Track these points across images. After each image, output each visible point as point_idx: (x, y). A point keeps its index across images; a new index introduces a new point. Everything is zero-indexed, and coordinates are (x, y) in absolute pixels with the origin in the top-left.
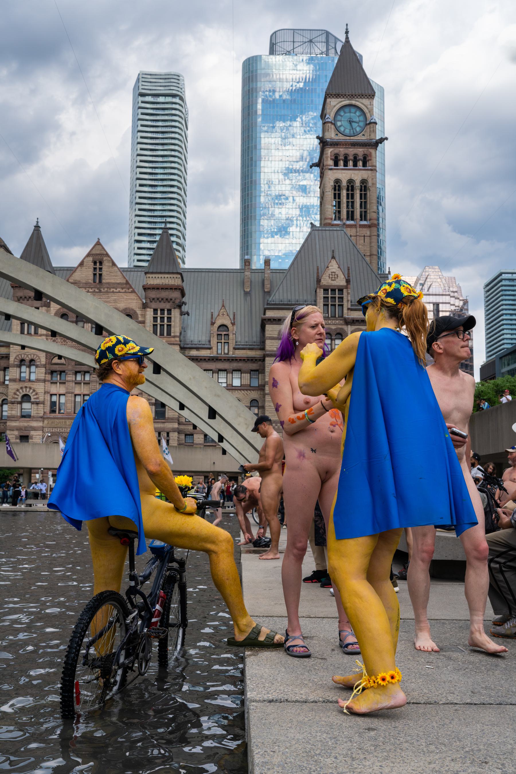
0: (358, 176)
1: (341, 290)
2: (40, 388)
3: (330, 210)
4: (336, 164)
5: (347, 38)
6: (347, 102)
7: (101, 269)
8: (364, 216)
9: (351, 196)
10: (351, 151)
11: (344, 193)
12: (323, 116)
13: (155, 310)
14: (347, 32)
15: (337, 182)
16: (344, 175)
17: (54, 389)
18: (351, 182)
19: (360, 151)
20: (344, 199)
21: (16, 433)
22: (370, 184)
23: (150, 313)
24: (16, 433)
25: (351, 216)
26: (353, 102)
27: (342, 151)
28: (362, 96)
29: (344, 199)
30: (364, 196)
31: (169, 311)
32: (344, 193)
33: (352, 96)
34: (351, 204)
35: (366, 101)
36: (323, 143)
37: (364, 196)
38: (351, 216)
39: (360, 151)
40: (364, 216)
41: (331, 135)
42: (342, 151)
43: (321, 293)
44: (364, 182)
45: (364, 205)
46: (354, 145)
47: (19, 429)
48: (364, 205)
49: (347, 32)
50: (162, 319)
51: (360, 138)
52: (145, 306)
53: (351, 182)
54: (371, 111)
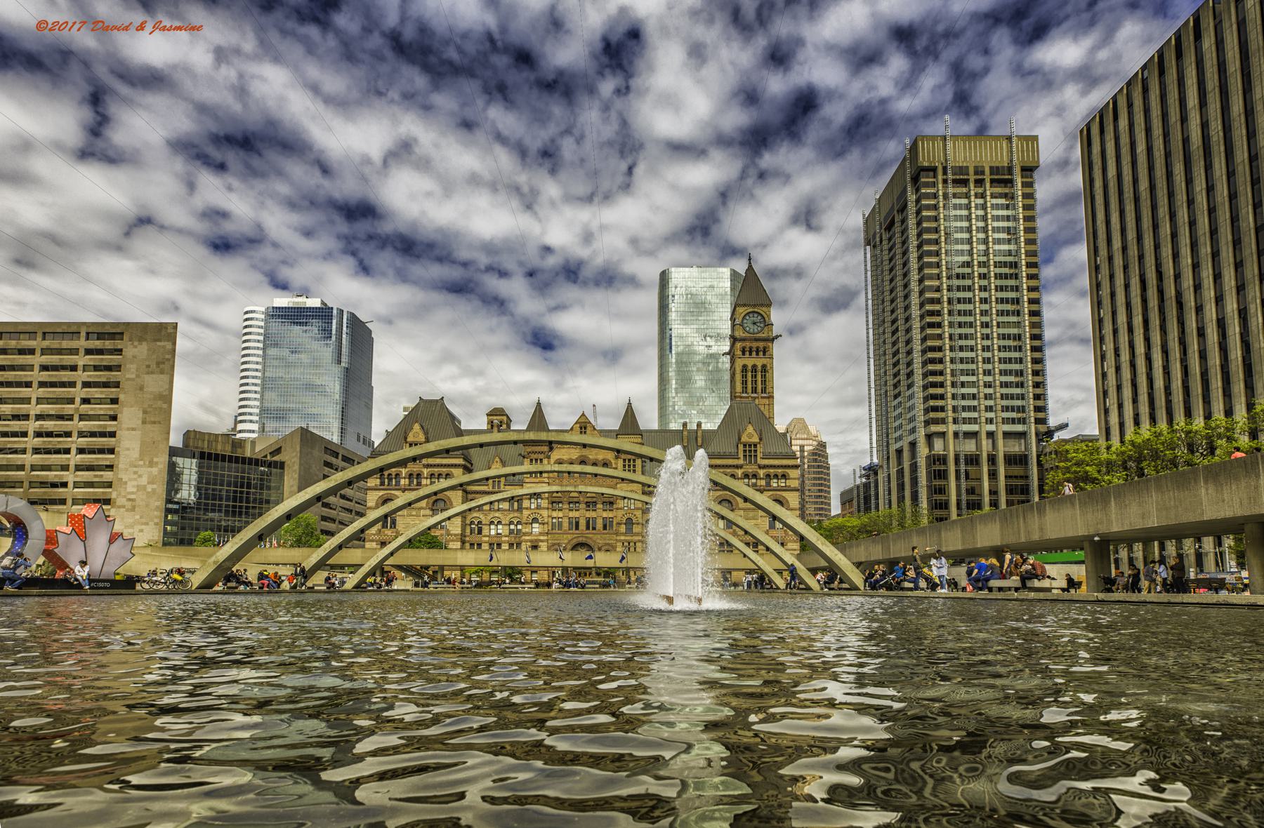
0: (760, 363)
1: (755, 446)
2: (545, 513)
3: (739, 387)
4: (744, 352)
8: (764, 391)
10: (755, 345)
11: (749, 374)
12: (733, 319)
15: (745, 366)
16: (750, 362)
17: (555, 514)
18: (754, 366)
20: (750, 379)
23: (620, 462)
25: (754, 390)
27: (748, 344)
28: (762, 305)
29: (750, 379)
30: (764, 376)
32: (749, 374)
33: (755, 306)
35: (765, 309)
36: (734, 340)
37: (764, 376)
38: (754, 390)
39: (761, 345)
40: (764, 391)
41: (739, 333)
42: (748, 344)
43: (741, 447)
44: (764, 366)
45: (764, 382)
46: (757, 340)
48: (764, 382)
51: (761, 335)
52: (617, 458)
53: (754, 366)
54: (769, 316)
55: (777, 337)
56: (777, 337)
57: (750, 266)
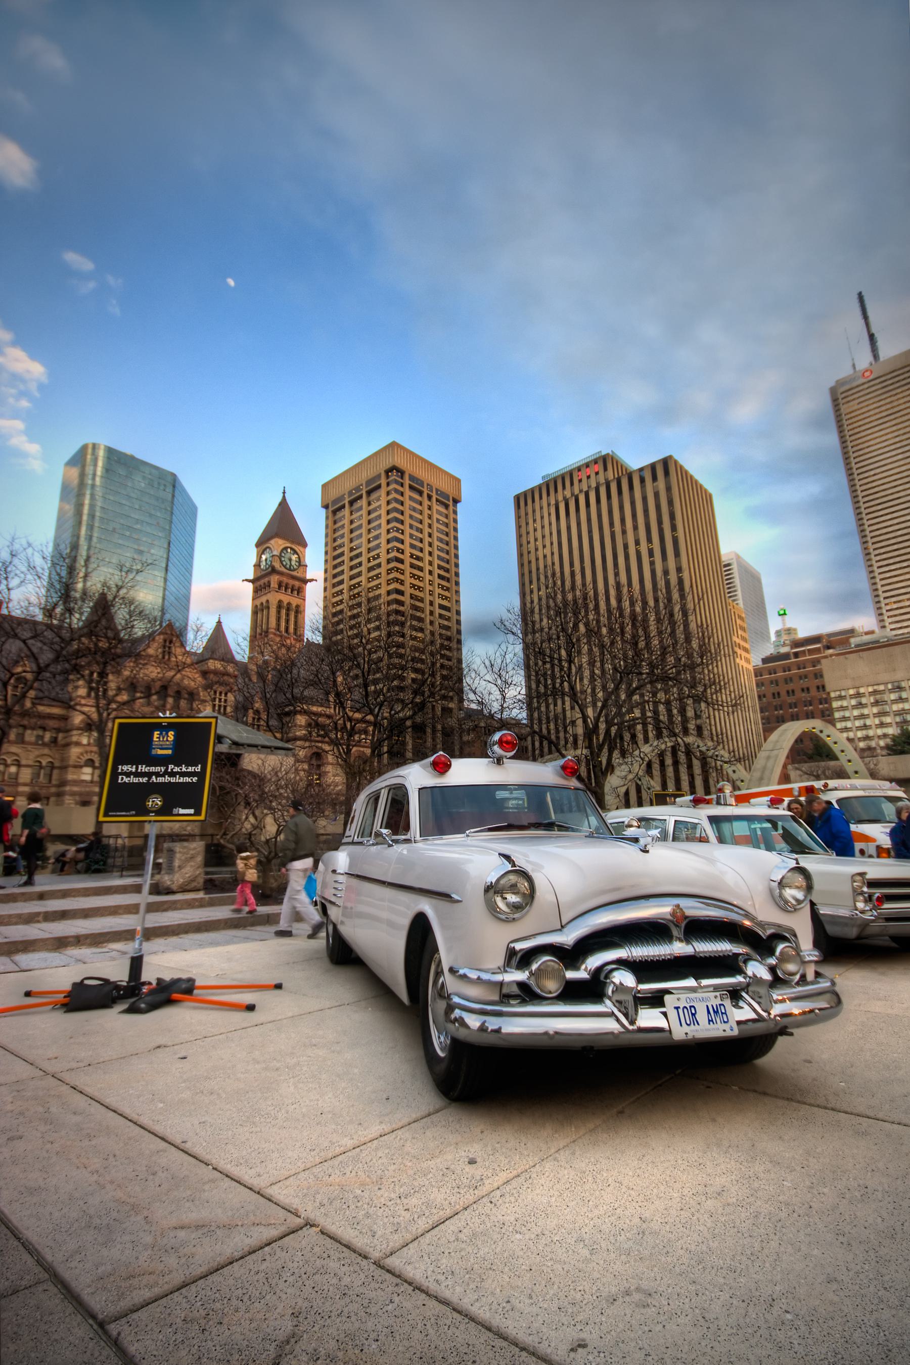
0: (295, 601)
5: (284, 496)
6: (289, 545)
7: (170, 648)
9: (288, 615)
11: (284, 612)
13: (215, 692)
14: (284, 493)
15: (280, 601)
16: (286, 598)
18: (289, 604)
19: (297, 584)
21: (77, 798)
22: (301, 609)
24: (77, 798)
26: (293, 547)
27: (285, 580)
31: (226, 694)
32: (284, 612)
33: (293, 542)
34: (287, 621)
35: (301, 549)
39: (297, 584)
44: (298, 606)
47: (80, 794)
49: (284, 493)
50: (220, 700)
51: (294, 573)
53: (289, 604)
54: (304, 557)
55: (311, 580)
56: (311, 580)
57: (284, 496)
